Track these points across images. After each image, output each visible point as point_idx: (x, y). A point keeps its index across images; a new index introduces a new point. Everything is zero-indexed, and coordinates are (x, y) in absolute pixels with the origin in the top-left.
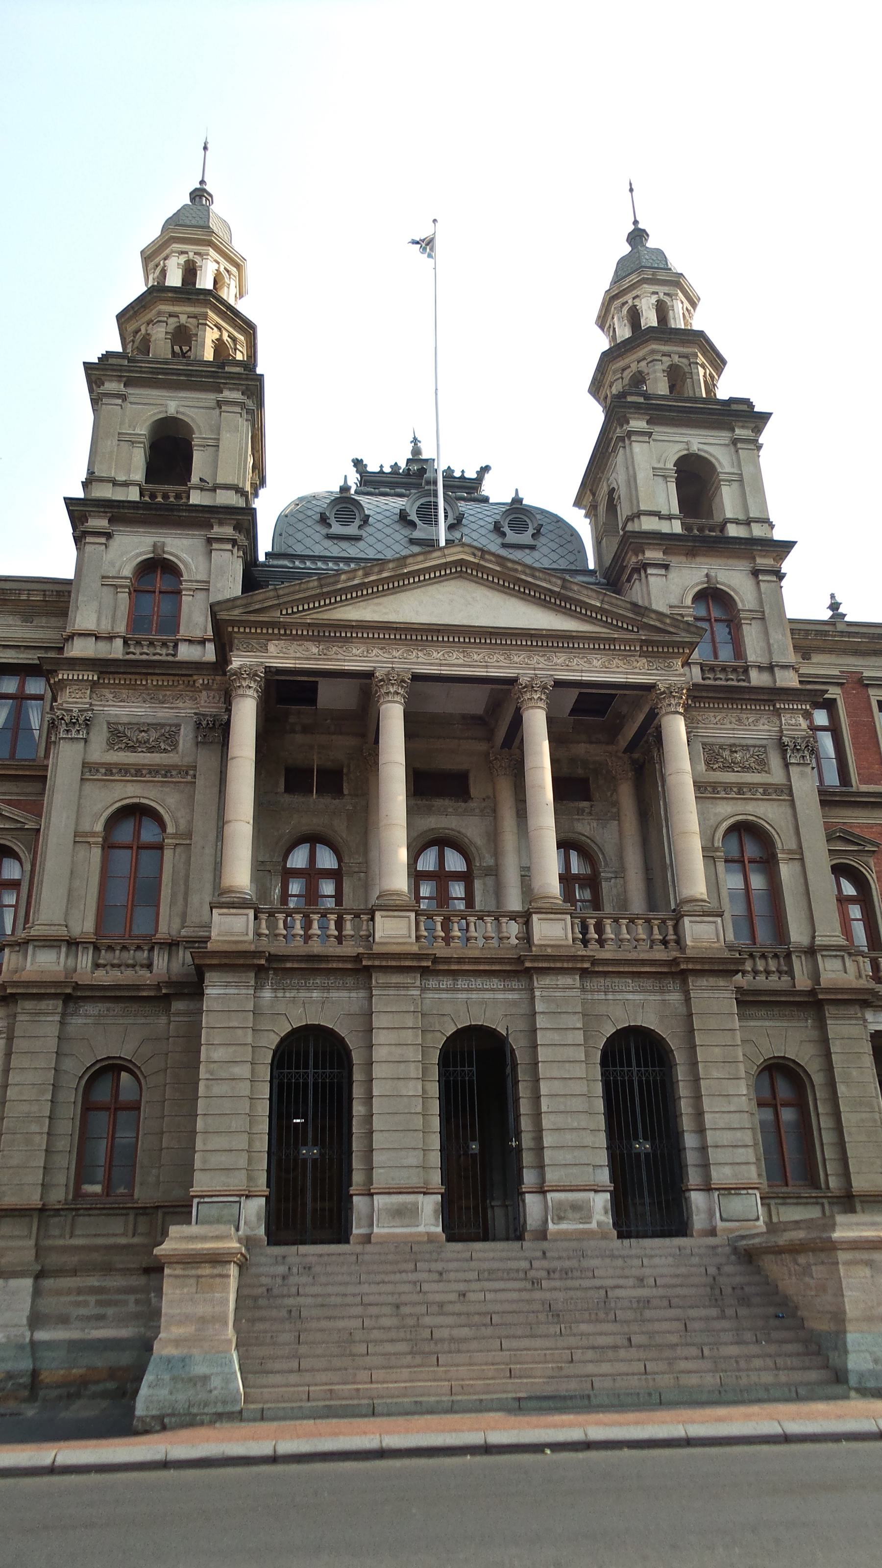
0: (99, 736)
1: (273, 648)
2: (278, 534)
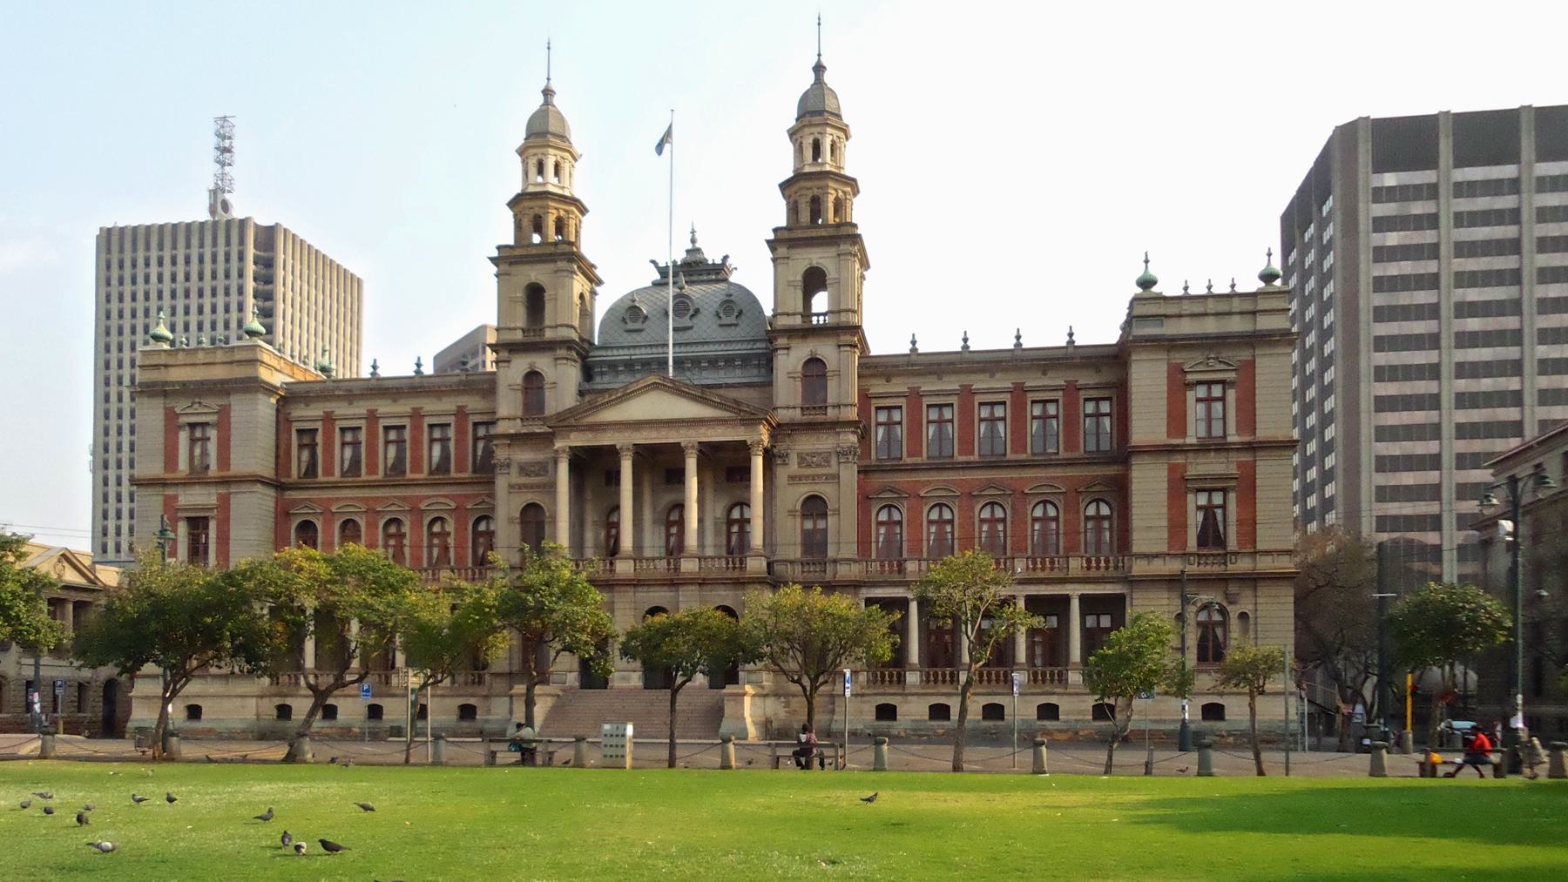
0: (514, 470)
2: (601, 333)
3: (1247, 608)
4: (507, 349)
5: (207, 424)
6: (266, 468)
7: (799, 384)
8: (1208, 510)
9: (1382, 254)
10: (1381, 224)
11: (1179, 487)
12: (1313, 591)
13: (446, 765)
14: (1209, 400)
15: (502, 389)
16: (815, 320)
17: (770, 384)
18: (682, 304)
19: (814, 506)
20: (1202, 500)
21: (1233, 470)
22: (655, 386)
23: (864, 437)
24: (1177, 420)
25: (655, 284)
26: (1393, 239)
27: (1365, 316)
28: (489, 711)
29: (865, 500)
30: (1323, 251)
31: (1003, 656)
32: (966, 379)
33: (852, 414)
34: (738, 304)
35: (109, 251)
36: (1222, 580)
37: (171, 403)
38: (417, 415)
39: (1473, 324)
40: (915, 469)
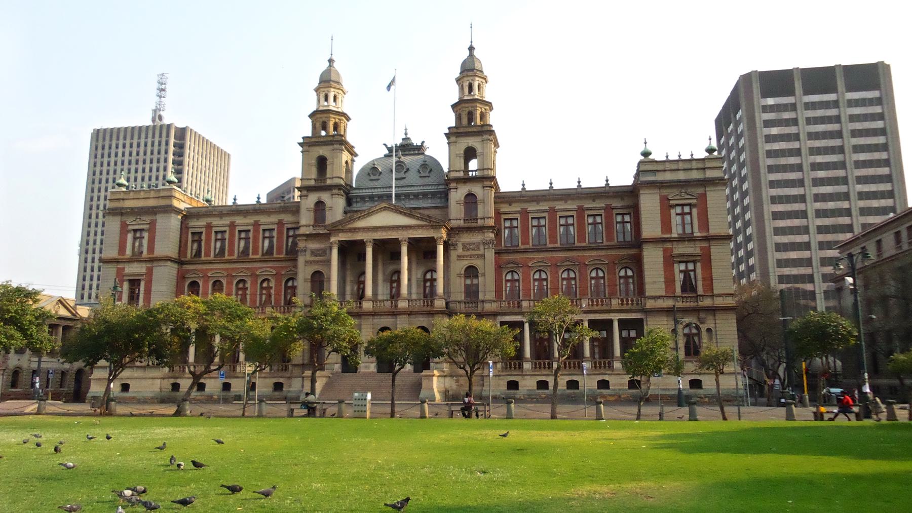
0: (308, 253)
1: (340, 235)
2: (356, 181)
3: (712, 326)
4: (306, 189)
5: (143, 230)
6: (173, 252)
7: (462, 207)
8: (686, 273)
9: (769, 139)
10: (768, 124)
11: (670, 260)
12: (747, 316)
13: (265, 417)
14: (683, 214)
15: (303, 210)
16: (470, 174)
17: (447, 207)
18: (400, 166)
19: (472, 272)
20: (683, 267)
21: (698, 251)
22: (385, 209)
23: (498, 234)
24: (666, 225)
25: (386, 156)
26: (774, 131)
27: (763, 170)
28: (290, 386)
29: (499, 268)
30: (739, 137)
31: (577, 353)
32: (552, 204)
33: (491, 222)
34: (430, 166)
35: (97, 140)
36: (696, 311)
37: (124, 219)
38: (256, 224)
39: (821, 174)
40: (526, 251)
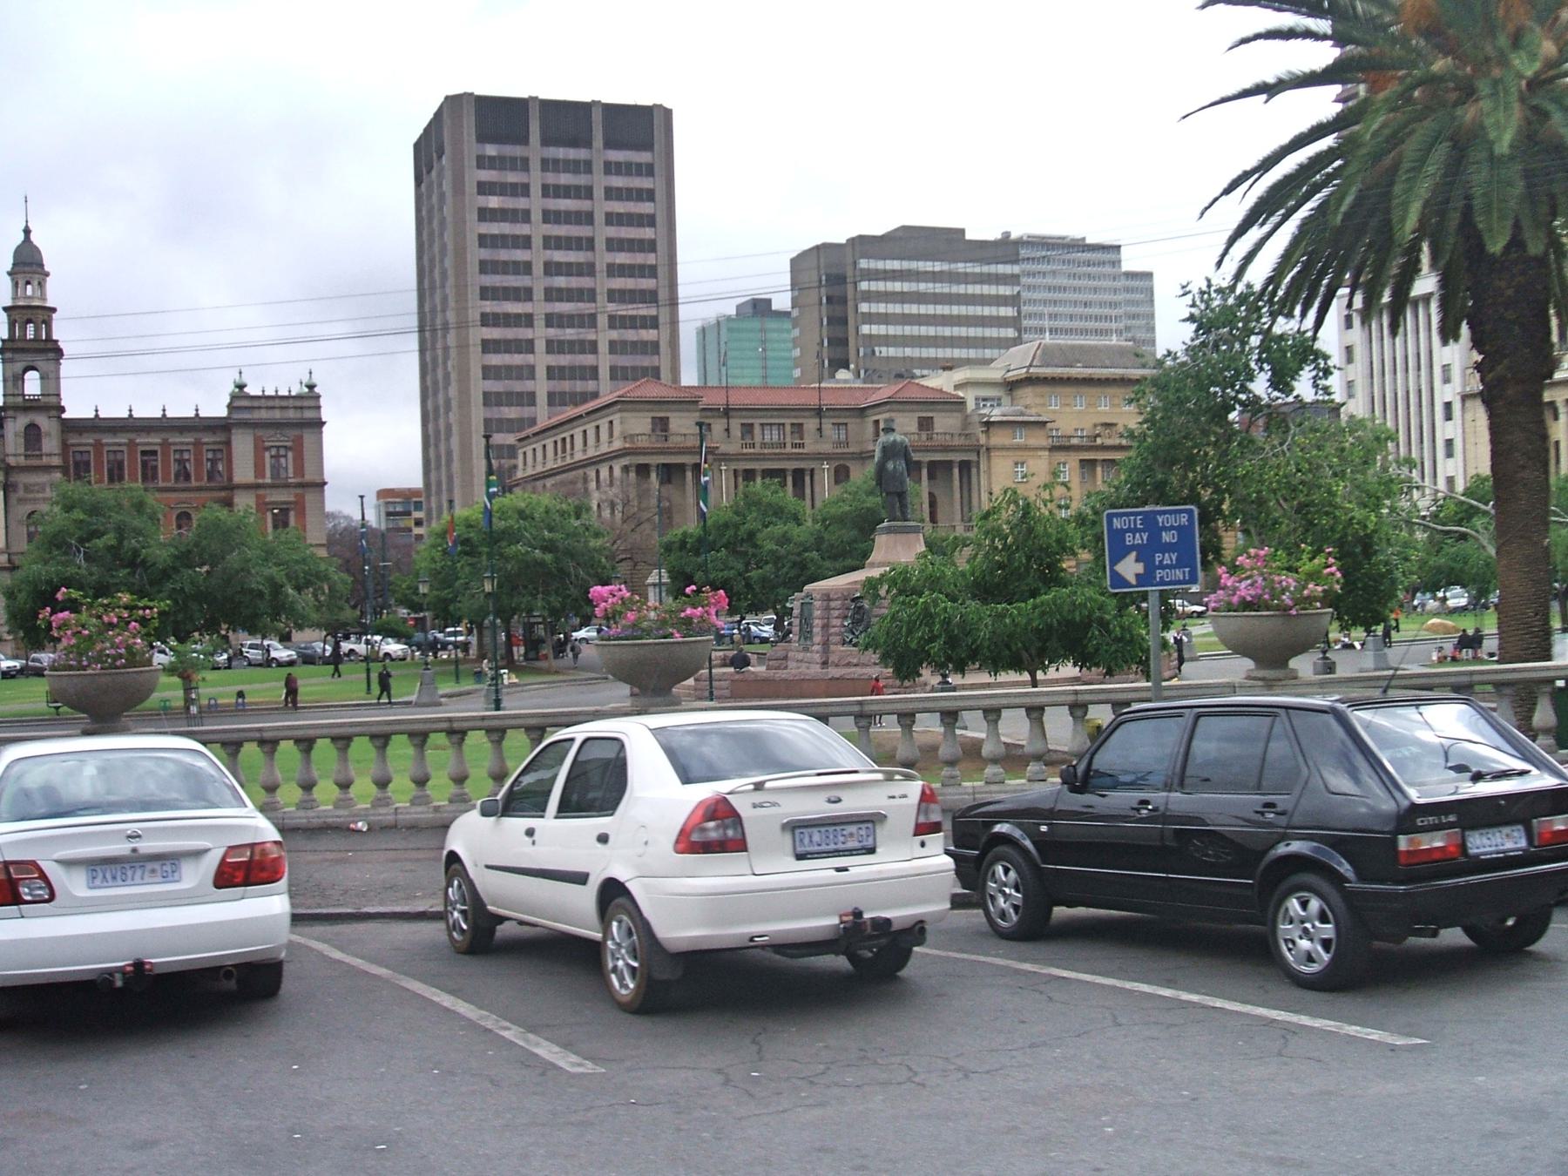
21: (292, 499)
33: (56, 461)
